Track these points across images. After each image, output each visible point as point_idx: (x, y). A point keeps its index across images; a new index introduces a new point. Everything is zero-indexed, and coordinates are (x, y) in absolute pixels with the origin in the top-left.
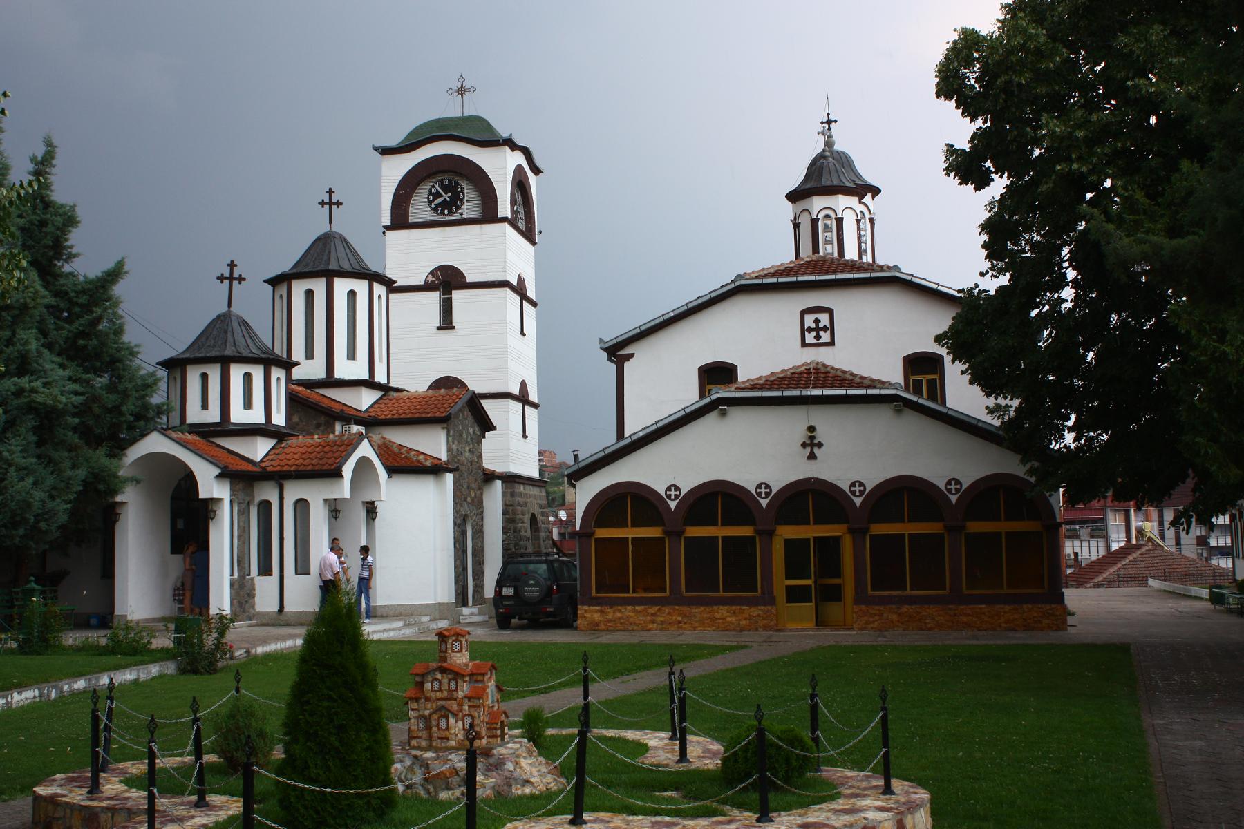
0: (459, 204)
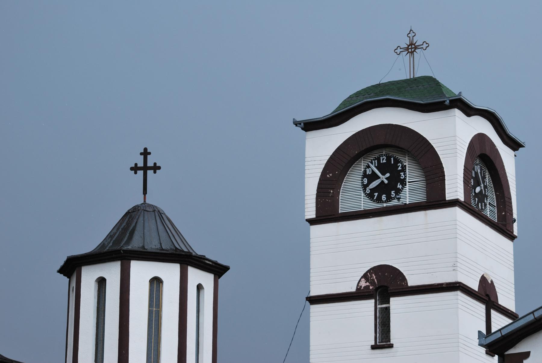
0: (399, 186)
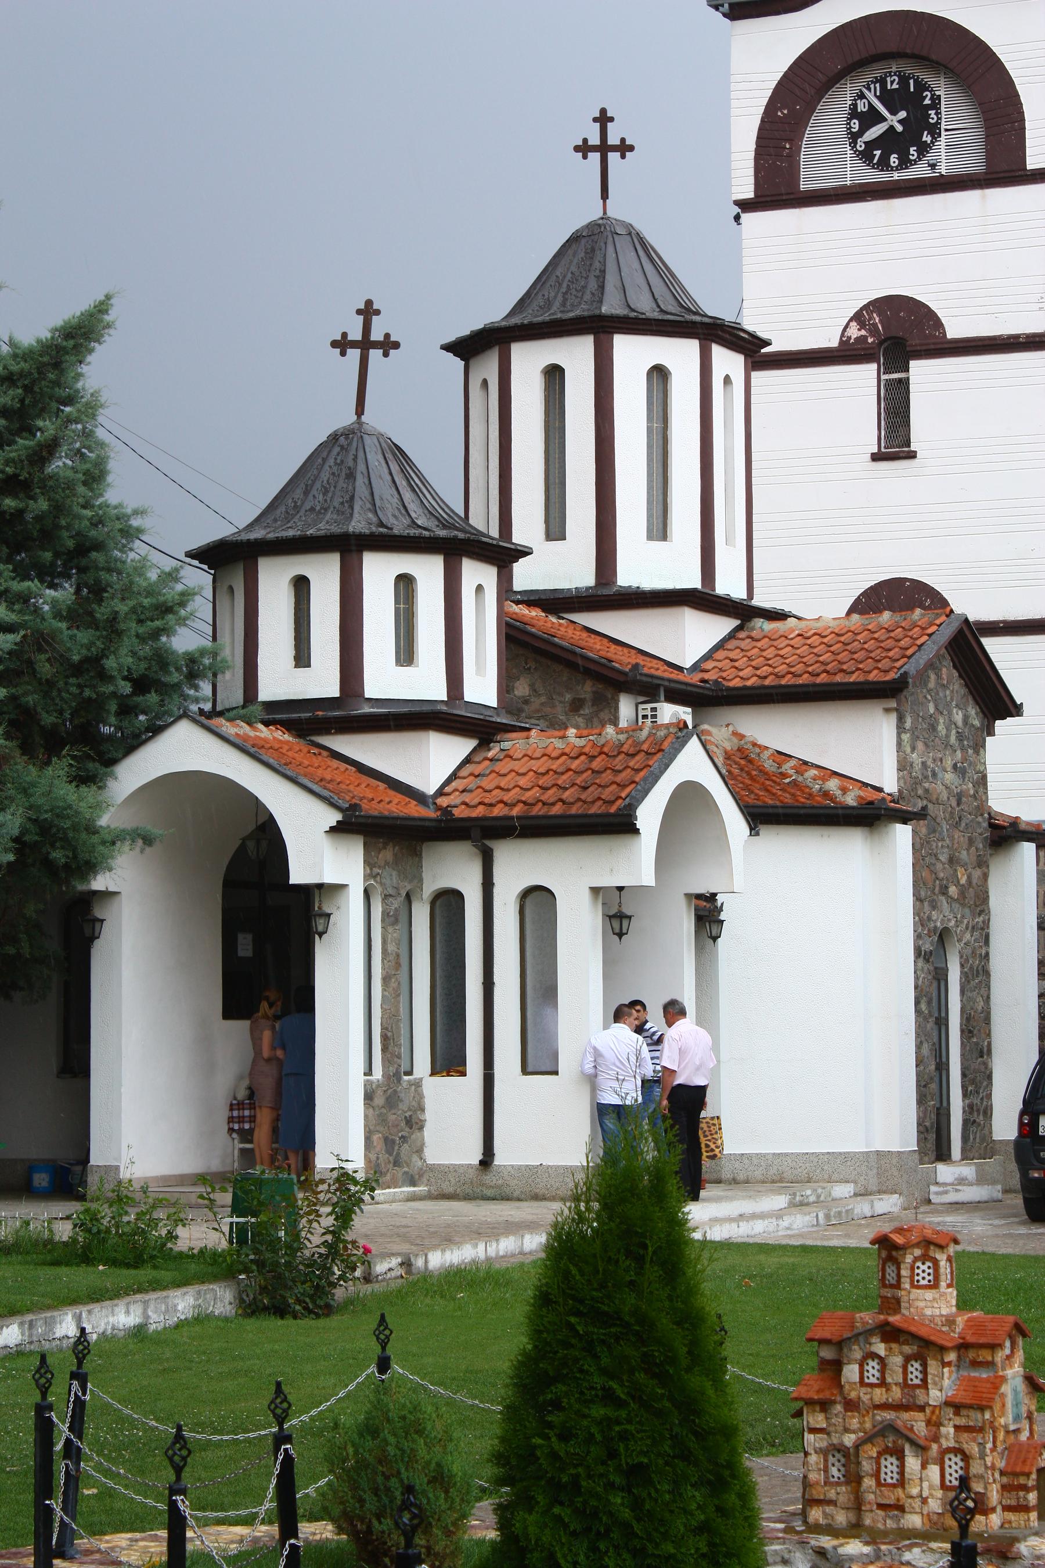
0: (927, 138)
